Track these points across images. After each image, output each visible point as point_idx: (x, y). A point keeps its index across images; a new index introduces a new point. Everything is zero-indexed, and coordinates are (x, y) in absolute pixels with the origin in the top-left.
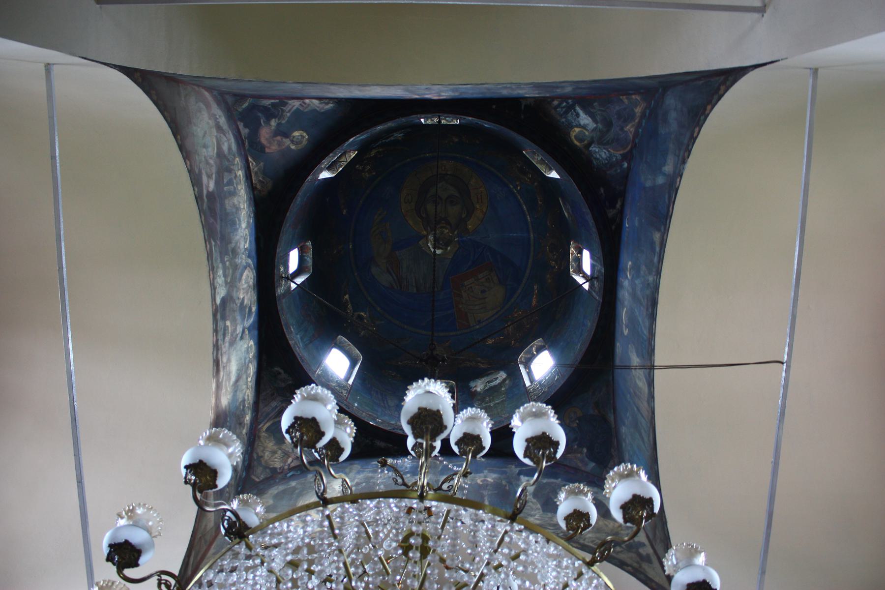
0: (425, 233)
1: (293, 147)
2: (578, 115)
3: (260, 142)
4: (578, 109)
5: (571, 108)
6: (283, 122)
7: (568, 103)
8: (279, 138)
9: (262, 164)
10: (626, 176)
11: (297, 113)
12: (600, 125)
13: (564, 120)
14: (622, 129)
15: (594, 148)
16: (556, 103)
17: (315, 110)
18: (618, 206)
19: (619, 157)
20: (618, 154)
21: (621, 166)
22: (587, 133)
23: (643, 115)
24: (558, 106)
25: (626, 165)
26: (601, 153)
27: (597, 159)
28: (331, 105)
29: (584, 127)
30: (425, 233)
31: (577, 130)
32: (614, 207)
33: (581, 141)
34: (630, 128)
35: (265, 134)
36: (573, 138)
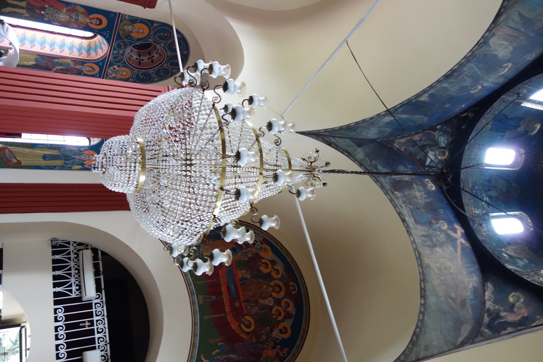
1: (522, 300)
3: (519, 320)
6: (502, 308)
7: (428, 169)
8: (515, 310)
9: (538, 317)
10: (447, 122)
11: (495, 302)
12: (428, 150)
14: (421, 140)
15: (443, 145)
17: (493, 293)
18: (465, 114)
19: (437, 132)
21: (441, 128)
22: (437, 153)
23: (402, 138)
25: (439, 127)
26: (443, 141)
27: (448, 140)
28: (489, 285)
29: (435, 155)
32: (467, 116)
33: (444, 153)
34: (417, 138)
35: (511, 318)
36: (446, 157)
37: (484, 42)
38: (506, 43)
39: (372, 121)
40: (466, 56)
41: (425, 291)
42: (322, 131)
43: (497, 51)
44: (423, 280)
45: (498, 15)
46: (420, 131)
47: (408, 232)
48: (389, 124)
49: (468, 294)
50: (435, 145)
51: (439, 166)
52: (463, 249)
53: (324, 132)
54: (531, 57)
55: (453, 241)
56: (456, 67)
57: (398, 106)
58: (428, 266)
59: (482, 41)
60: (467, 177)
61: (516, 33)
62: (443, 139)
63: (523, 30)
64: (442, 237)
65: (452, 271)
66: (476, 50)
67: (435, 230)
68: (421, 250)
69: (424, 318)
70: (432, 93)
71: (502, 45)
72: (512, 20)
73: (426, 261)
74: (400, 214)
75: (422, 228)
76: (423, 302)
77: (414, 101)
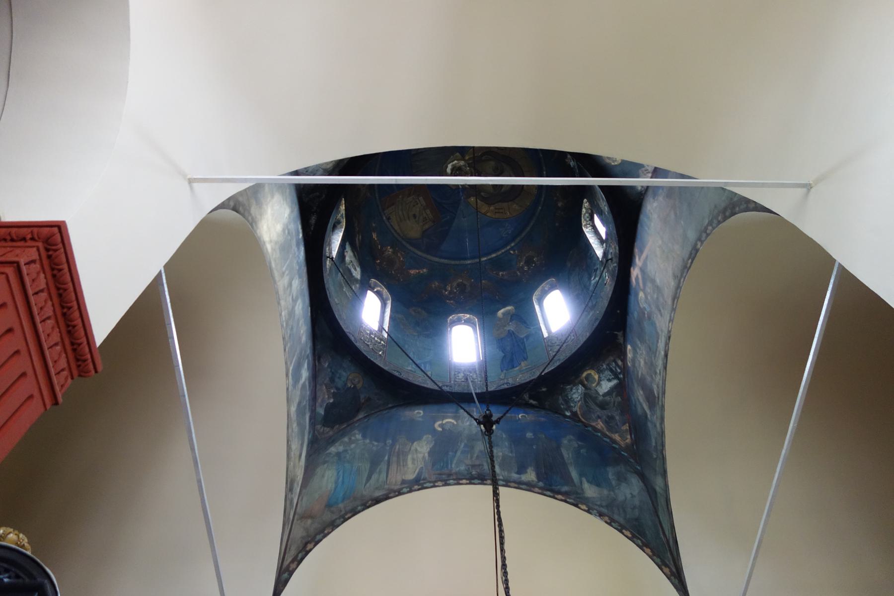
0: (467, 158)
2: (609, 380)
4: (615, 382)
5: (616, 376)
10: (557, 411)
12: (601, 398)
13: (605, 366)
14: (599, 417)
15: (581, 388)
16: (620, 363)
18: (532, 401)
19: (574, 410)
20: (576, 409)
21: (567, 410)
23: (614, 442)
24: (617, 365)
25: (568, 414)
26: (576, 394)
27: (571, 390)
29: (599, 384)
30: (467, 158)
31: (596, 377)
32: (530, 398)
33: (587, 378)
34: (600, 425)
36: (589, 372)
37: (418, 484)
38: (410, 457)
39: (604, 510)
40: (443, 485)
41: (691, 254)
42: (667, 570)
43: (424, 457)
44: (686, 268)
45: (377, 501)
46: (590, 429)
47: (669, 338)
48: (596, 482)
49: (661, 198)
50: (589, 396)
51: (605, 366)
52: (641, 252)
53: (667, 566)
54: (418, 413)
55: (643, 271)
56: (464, 481)
57: (560, 497)
58: (675, 277)
59: (416, 487)
60: (498, 381)
61: (394, 459)
62: (575, 396)
63: (386, 458)
64: (649, 288)
65: (660, 242)
66: (430, 482)
67: (650, 306)
68: (670, 302)
69: (708, 225)
70: (519, 473)
71: (413, 459)
72: (378, 480)
73: (673, 284)
74: (665, 368)
75: (657, 322)
76: (699, 244)
77: (541, 484)
